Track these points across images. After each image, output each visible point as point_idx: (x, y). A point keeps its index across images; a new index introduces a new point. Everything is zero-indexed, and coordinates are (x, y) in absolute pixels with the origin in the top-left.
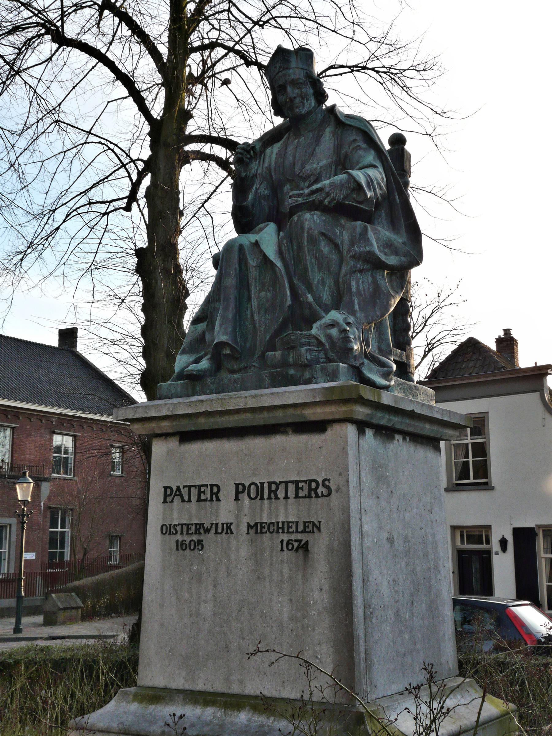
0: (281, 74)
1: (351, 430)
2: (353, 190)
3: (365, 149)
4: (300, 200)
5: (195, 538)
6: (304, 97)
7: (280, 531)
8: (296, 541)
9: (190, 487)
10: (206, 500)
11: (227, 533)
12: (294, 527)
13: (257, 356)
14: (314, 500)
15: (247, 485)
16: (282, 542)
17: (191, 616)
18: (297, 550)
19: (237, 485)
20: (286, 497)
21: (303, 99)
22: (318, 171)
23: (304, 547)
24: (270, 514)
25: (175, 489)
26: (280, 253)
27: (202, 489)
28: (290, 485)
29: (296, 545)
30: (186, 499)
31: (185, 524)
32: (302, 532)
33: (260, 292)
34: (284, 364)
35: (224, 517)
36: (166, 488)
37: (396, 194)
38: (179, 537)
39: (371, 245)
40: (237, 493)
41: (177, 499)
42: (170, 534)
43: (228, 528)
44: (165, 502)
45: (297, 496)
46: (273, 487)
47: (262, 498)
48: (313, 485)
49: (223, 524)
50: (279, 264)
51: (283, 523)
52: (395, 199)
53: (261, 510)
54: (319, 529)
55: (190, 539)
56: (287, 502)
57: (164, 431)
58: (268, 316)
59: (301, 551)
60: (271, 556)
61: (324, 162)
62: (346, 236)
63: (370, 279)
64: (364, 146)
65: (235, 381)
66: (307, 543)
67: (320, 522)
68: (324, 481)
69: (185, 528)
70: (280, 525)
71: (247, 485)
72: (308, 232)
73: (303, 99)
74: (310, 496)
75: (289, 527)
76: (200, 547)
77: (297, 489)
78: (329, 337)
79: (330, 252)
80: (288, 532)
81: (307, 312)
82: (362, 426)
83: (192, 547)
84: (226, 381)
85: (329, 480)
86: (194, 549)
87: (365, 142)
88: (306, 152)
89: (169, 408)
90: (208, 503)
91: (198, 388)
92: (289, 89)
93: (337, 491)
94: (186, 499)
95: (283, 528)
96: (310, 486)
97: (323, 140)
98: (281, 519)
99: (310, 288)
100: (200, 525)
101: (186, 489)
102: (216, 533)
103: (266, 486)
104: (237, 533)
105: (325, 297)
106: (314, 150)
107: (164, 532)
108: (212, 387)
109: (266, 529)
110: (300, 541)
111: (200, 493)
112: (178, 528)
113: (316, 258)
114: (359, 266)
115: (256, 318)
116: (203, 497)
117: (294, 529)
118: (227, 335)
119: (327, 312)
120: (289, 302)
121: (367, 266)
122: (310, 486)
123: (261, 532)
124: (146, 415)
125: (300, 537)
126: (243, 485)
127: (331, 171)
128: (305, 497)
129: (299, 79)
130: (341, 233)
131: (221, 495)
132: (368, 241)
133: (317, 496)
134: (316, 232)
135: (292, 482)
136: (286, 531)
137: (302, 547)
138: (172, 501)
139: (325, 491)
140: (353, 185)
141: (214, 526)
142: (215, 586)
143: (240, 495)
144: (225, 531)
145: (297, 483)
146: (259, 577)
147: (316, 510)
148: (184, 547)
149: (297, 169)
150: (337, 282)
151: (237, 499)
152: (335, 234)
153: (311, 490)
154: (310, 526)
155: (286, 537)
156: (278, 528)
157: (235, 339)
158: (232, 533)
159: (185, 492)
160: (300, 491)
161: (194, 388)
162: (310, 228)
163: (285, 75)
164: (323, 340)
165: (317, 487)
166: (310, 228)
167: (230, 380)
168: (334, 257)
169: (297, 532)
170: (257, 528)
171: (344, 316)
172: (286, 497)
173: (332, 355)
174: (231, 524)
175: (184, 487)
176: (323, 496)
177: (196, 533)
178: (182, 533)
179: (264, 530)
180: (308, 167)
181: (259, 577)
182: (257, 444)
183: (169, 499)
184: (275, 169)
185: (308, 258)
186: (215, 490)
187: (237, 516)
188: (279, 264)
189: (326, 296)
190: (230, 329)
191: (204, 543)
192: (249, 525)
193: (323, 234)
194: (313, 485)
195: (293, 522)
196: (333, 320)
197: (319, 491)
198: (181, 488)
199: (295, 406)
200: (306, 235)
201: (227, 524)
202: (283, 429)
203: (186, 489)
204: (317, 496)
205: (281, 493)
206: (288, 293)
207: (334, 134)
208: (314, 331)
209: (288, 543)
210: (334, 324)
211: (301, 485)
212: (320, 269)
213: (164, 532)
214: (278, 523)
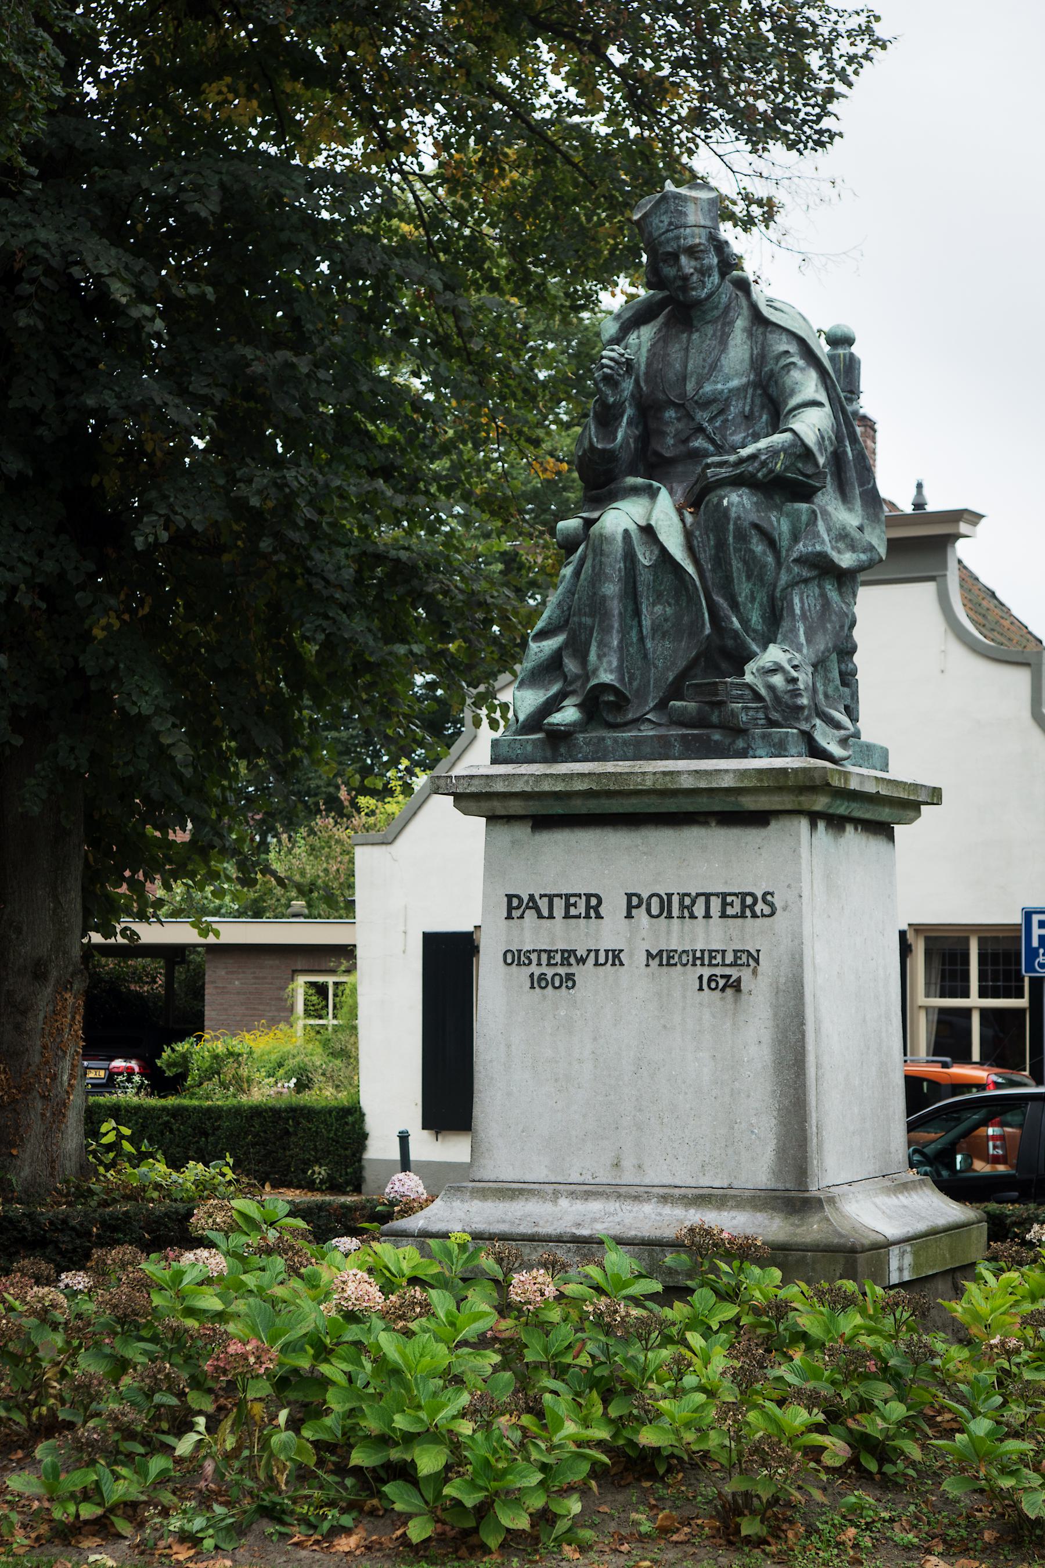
0: (670, 235)
1: (804, 824)
2: (799, 457)
3: (802, 370)
4: (724, 472)
5: (562, 971)
6: (704, 272)
7: (698, 962)
8: (722, 976)
9: (551, 898)
10: (579, 917)
11: (614, 964)
13: (652, 705)
15: (645, 896)
16: (701, 977)
17: (556, 1080)
18: (723, 990)
19: (629, 896)
20: (707, 916)
21: (703, 275)
22: (725, 396)
23: (736, 986)
24: (682, 937)
25: (526, 899)
26: (690, 548)
27: (572, 900)
28: (712, 898)
30: (546, 913)
31: (545, 951)
32: (730, 965)
33: (654, 605)
34: (700, 722)
36: (510, 897)
37: (847, 444)
38: (537, 972)
39: (823, 542)
40: (630, 907)
41: (530, 914)
42: (519, 964)
43: (615, 957)
44: (509, 917)
45: (724, 915)
46: (687, 901)
47: (670, 916)
48: (749, 900)
50: (690, 569)
52: (845, 452)
53: (669, 932)
56: (708, 925)
57: (512, 812)
58: (667, 644)
60: (684, 997)
61: (735, 383)
62: (785, 526)
63: (817, 591)
64: (801, 363)
66: (739, 980)
67: (758, 951)
69: (544, 957)
70: (698, 954)
71: (645, 896)
72: (735, 524)
73: (703, 275)
74: (743, 916)
75: (711, 958)
76: (570, 984)
77: (724, 904)
78: (771, 688)
79: (764, 553)
80: (710, 965)
81: (730, 643)
82: (814, 817)
83: (557, 984)
85: (772, 894)
86: (560, 987)
87: (802, 358)
88: (704, 360)
89: (527, 782)
90: (582, 921)
91: (562, 750)
92: (683, 259)
93: (785, 909)
94: (546, 913)
95: (702, 958)
96: (743, 901)
97: (731, 343)
98: (699, 947)
99: (735, 605)
100: (569, 952)
101: (546, 899)
102: (596, 964)
103: (675, 899)
104: (630, 965)
105: (754, 619)
107: (509, 961)
108: (586, 749)
111: (568, 906)
112: (534, 957)
113: (745, 562)
114: (806, 573)
115: (649, 645)
116: (573, 911)
118: (611, 672)
119: (765, 648)
120: (708, 631)
121: (814, 573)
122: (743, 901)
123: (668, 964)
124: (488, 790)
125: (727, 971)
126: (638, 896)
127: (745, 398)
129: (700, 244)
130: (779, 521)
131: (602, 910)
132: (817, 535)
134: (746, 524)
135: (717, 895)
136: (706, 962)
137: (731, 986)
138: (522, 917)
139: (767, 910)
140: (799, 450)
141: (592, 954)
142: (595, 1039)
143: (634, 912)
144: (610, 961)
145: (724, 896)
146: (665, 1027)
147: (750, 934)
148: (543, 984)
149: (690, 386)
150: (772, 599)
151: (629, 916)
152: (771, 523)
153: (748, 906)
154: (744, 957)
155: (707, 972)
156: (695, 958)
157: (621, 680)
158: (622, 964)
159: (543, 905)
160: (729, 908)
162: (739, 518)
163: (678, 238)
164: (763, 692)
165: (755, 902)
166: (739, 518)
168: (770, 559)
169: (724, 965)
170: (663, 958)
171: (789, 656)
172: (707, 916)
173: (775, 716)
174: (621, 951)
175: (541, 896)
177: (562, 964)
178: (539, 964)
179: (672, 962)
180: (708, 388)
182: (663, 841)
183: (516, 913)
184: (646, 374)
185: (734, 562)
186: (594, 902)
187: (629, 941)
188: (690, 569)
189: (755, 618)
190: (615, 664)
193: (756, 526)
194: (749, 900)
195: (717, 951)
196: (775, 663)
197: (758, 909)
198: (537, 898)
199: (728, 790)
200: (731, 527)
201: (614, 951)
202: (702, 819)
203: (546, 899)
204: (754, 916)
205: (699, 909)
206: (706, 615)
207: (751, 334)
208: (748, 678)
209: (710, 980)
210: (777, 669)
211: (729, 899)
212: (749, 578)
213: (509, 961)
214: (694, 951)
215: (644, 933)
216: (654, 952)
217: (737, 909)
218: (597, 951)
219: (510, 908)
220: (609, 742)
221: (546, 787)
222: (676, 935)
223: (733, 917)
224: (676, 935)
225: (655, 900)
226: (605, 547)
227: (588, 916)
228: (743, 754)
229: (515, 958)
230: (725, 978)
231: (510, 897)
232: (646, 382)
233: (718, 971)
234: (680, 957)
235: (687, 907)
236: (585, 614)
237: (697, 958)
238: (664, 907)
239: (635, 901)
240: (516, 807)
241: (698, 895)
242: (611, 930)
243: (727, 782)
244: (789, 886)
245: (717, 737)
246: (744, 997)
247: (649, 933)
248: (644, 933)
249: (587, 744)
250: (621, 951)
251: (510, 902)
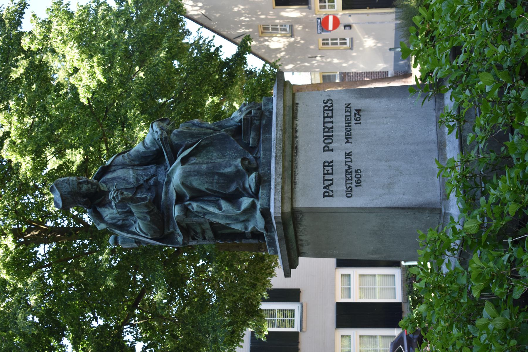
5: (354, 174)
7: (350, 125)
8: (355, 116)
9: (325, 180)
10: (332, 169)
12: (348, 117)
14: (334, 108)
15: (325, 145)
16: (356, 123)
18: (360, 116)
19: (324, 151)
20: (332, 122)
23: (359, 111)
25: (325, 190)
28: (325, 121)
29: (357, 116)
30: (331, 182)
34: (258, 130)
35: (342, 158)
36: (325, 196)
40: (329, 150)
41: (331, 188)
42: (351, 191)
43: (348, 155)
44: (332, 196)
45: (332, 117)
46: (326, 130)
47: (332, 136)
49: (346, 158)
51: (346, 123)
53: (339, 136)
54: (349, 104)
55: (354, 178)
59: (361, 113)
65: (264, 155)
66: (356, 110)
68: (324, 103)
69: (348, 182)
70: (347, 125)
71: (325, 145)
74: (332, 110)
75: (348, 120)
76: (359, 171)
77: (328, 117)
80: (351, 120)
83: (359, 176)
84: (264, 161)
91: (266, 178)
94: (331, 182)
95: (348, 123)
96: (327, 110)
98: (344, 125)
102: (351, 162)
103: (325, 134)
106: (121, 179)
107: (350, 195)
108: (266, 169)
110: (355, 114)
111: (328, 174)
112: (348, 186)
117: (349, 117)
122: (327, 110)
123: (351, 135)
124: (280, 193)
125: (353, 114)
128: (332, 112)
131: (330, 160)
133: (332, 106)
135: (324, 119)
137: (359, 113)
138: (332, 191)
139: (330, 102)
141: (347, 163)
143: (330, 149)
145: (324, 117)
146: (375, 136)
148: (359, 181)
151: (332, 150)
155: (353, 122)
156: (348, 126)
158: (351, 152)
159: (327, 183)
161: (265, 181)
167: (263, 158)
169: (350, 116)
170: (348, 137)
172: (332, 122)
174: (346, 153)
175: (324, 184)
176: (332, 103)
178: (351, 183)
180: (131, 180)
181: (375, 136)
183: (331, 193)
184: (122, 209)
192: (347, 142)
194: (326, 108)
201: (346, 155)
203: (325, 182)
204: (332, 106)
209: (357, 120)
211: (326, 115)
213: (350, 195)
214: (346, 126)
215: (339, 145)
216: (346, 141)
217: (330, 112)
218: (346, 162)
221: (280, 170)
222: (339, 133)
224: (339, 133)
225: (326, 141)
226: (187, 171)
228: (271, 113)
229: (349, 193)
230: (355, 115)
231: (324, 196)
232: (125, 209)
233: (353, 118)
236: (213, 180)
240: (288, 188)
241: (324, 126)
242: (338, 157)
243: (281, 105)
245: (264, 122)
246: (362, 109)
247: (339, 144)
248: (339, 145)
249: (264, 169)
251: (327, 196)
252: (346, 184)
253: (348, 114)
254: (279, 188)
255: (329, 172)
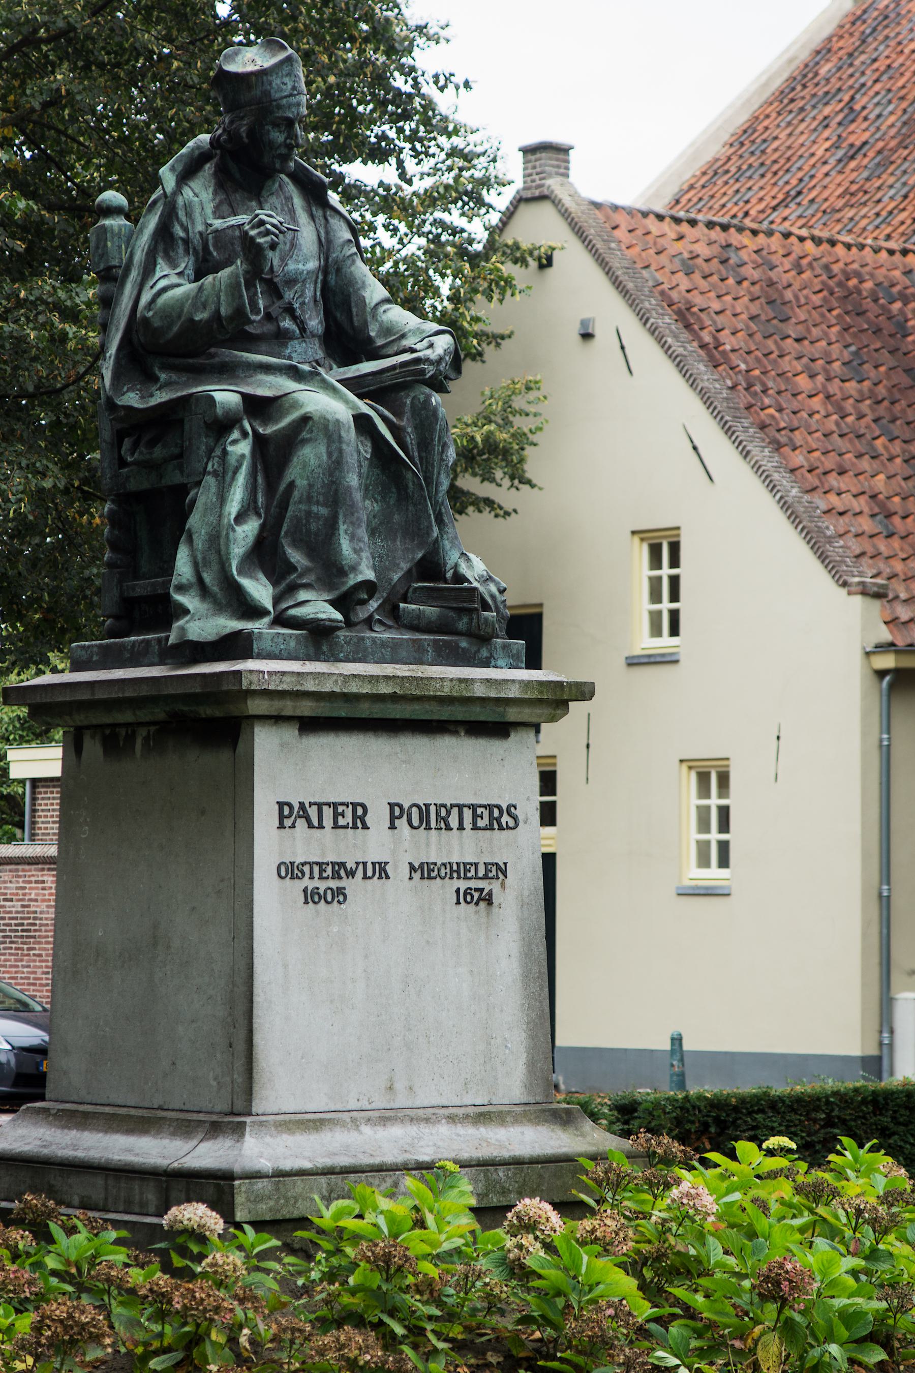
5: (333, 884)
7: (455, 875)
8: (476, 890)
9: (320, 806)
10: (346, 827)
11: (380, 878)
12: (473, 869)
16: (458, 891)
17: (332, 1002)
18: (477, 904)
19: (392, 806)
20: (461, 828)
23: (488, 900)
25: (296, 807)
28: (465, 810)
29: (476, 895)
30: (316, 823)
31: (317, 863)
36: (281, 805)
38: (311, 885)
40: (393, 818)
41: (301, 823)
43: (381, 870)
44: (281, 826)
45: (475, 827)
46: (443, 812)
47: (428, 828)
53: (428, 845)
55: (326, 883)
59: (482, 904)
60: (444, 911)
66: (490, 894)
67: (505, 864)
68: (509, 807)
69: (316, 869)
70: (455, 868)
76: (341, 898)
77: (475, 816)
80: (466, 878)
83: (329, 899)
89: (336, 681)
91: (325, 648)
94: (316, 823)
95: (458, 872)
98: (454, 859)
100: (338, 864)
102: (365, 877)
103: (433, 809)
107: (283, 874)
108: (347, 648)
109: (436, 872)
110: (481, 890)
111: (336, 815)
112: (306, 869)
116: (341, 821)
117: (472, 873)
123: (429, 878)
124: (299, 688)
125: (480, 884)
126: (401, 807)
138: (293, 826)
139: (511, 823)
142: (366, 957)
143: (397, 822)
144: (377, 875)
145: (474, 807)
146: (428, 942)
148: (316, 898)
151: (392, 827)
155: (463, 885)
158: (388, 877)
159: (313, 812)
170: (424, 871)
172: (461, 828)
174: (386, 863)
175: (311, 804)
181: (428, 942)
183: (288, 822)
191: (346, 892)
192: (412, 868)
194: (496, 813)
198: (307, 805)
201: (380, 864)
202: (452, 727)
203: (315, 808)
204: (501, 828)
205: (454, 821)
209: (465, 894)
211: (479, 810)
213: (283, 874)
215: (406, 845)
216: (416, 865)
218: (365, 864)
219: (282, 817)
220: (368, 643)
221: (354, 688)
223: (484, 829)
225: (415, 810)
226: (343, 434)
227: (355, 827)
228: (486, 664)
229: (290, 871)
230: (477, 889)
231: (281, 805)
232: (215, 246)
233: (473, 884)
234: (439, 870)
235: (359, 817)
236: (318, 503)
237: (460, 870)
238: (429, 817)
239: (397, 811)
241: (452, 806)
243: (513, 692)
244: (528, 799)
245: (464, 644)
246: (495, 909)
248: (406, 845)
249: (348, 643)
250: (386, 863)
252: (311, 864)
253: (481, 873)
254: (310, 686)
255: (340, 818)
